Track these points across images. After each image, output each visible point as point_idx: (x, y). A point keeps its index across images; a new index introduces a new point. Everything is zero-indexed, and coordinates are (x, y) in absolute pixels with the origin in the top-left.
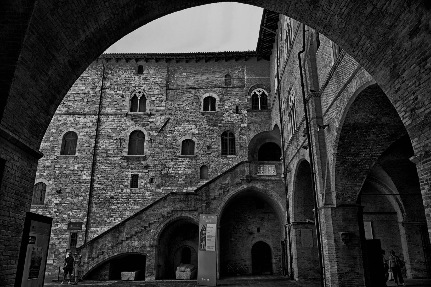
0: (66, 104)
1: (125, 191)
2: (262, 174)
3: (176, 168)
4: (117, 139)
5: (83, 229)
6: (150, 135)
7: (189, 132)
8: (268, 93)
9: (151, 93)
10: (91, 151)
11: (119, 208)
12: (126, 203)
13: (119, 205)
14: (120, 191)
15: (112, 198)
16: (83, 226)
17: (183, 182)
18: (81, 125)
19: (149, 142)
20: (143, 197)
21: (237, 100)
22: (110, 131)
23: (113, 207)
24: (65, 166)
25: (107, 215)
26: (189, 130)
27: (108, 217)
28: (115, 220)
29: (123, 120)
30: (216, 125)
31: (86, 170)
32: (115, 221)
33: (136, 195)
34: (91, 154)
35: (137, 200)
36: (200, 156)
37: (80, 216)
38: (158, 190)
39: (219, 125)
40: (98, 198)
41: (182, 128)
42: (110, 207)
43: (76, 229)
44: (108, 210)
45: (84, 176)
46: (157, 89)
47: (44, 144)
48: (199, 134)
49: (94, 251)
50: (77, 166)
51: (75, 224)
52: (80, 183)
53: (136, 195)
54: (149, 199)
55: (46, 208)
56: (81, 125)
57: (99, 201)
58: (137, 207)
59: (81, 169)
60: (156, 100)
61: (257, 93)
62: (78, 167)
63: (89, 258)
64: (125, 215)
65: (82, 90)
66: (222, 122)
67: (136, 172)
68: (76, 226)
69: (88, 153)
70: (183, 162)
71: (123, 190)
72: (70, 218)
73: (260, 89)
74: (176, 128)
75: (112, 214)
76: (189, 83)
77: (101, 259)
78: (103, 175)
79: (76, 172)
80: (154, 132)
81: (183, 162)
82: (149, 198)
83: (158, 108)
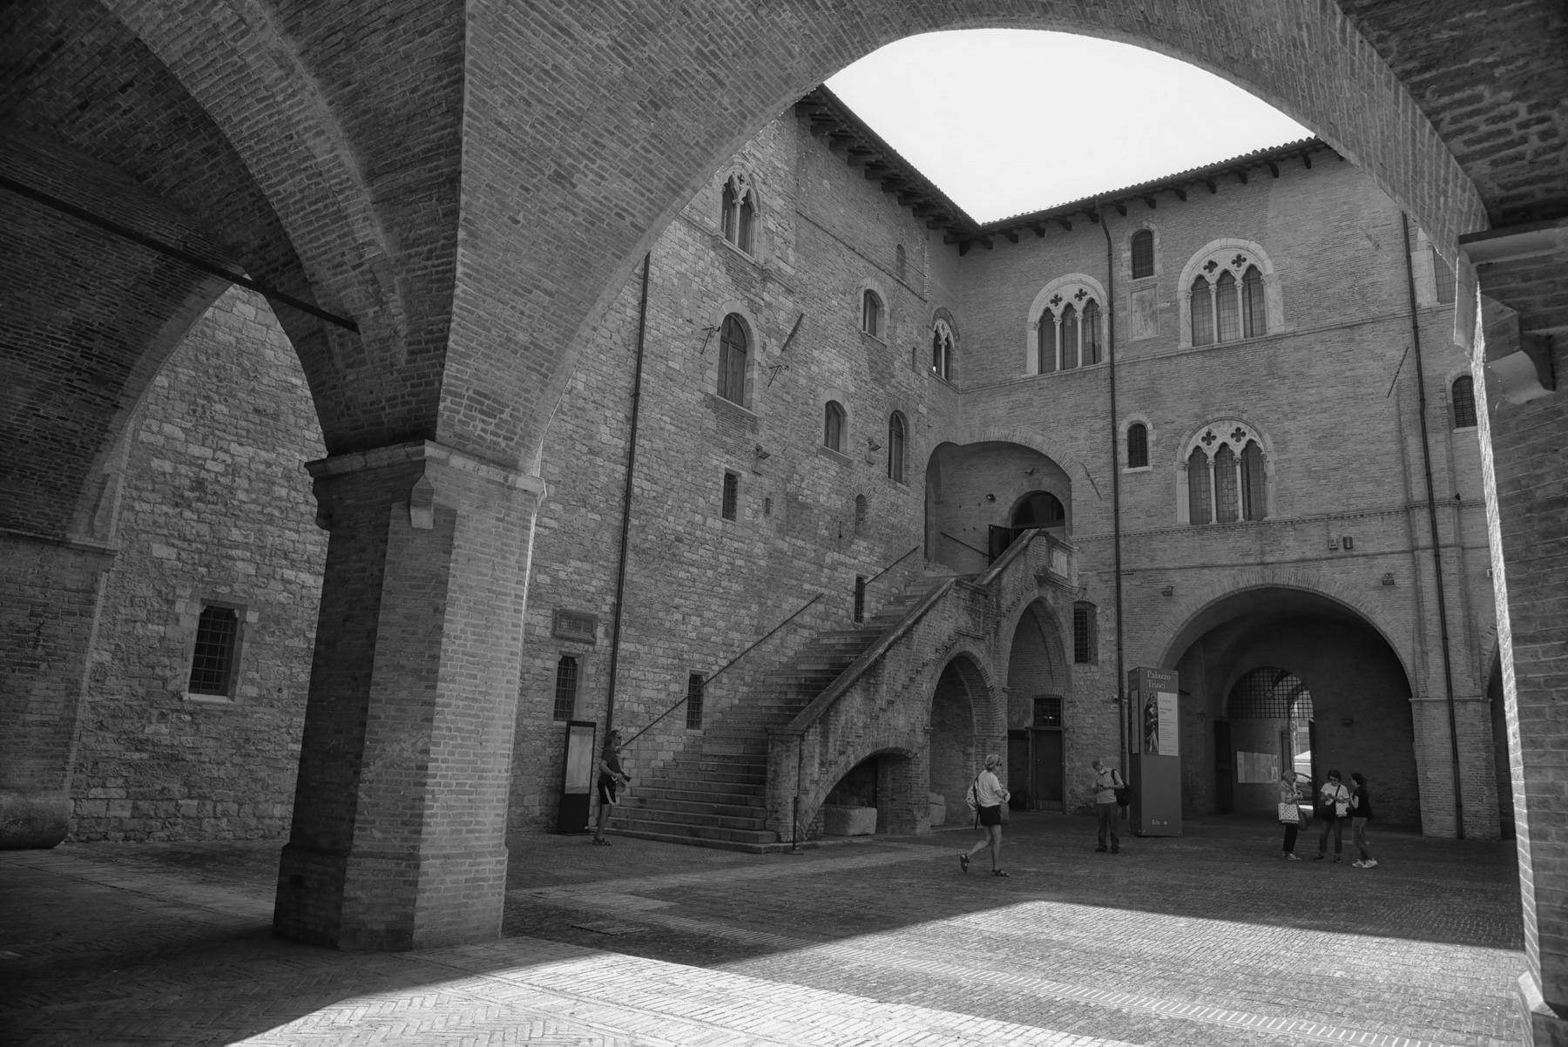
1: (710, 521)
4: (690, 321)
5: (599, 641)
6: (764, 348)
7: (839, 381)
9: (766, 199)
10: (624, 334)
13: (695, 571)
14: (698, 518)
15: (679, 540)
16: (600, 631)
17: (826, 533)
19: (763, 372)
20: (748, 556)
22: (675, 281)
25: (666, 600)
27: (668, 608)
30: (883, 387)
31: (611, 405)
32: (683, 628)
33: (736, 545)
35: (738, 562)
37: (592, 589)
38: (780, 544)
42: (674, 572)
43: (579, 641)
44: (668, 582)
45: (603, 428)
48: (853, 395)
49: (831, 739)
52: (591, 452)
53: (736, 545)
57: (646, 540)
58: (736, 587)
59: (597, 397)
63: (822, 764)
67: (735, 468)
68: (577, 628)
69: (616, 337)
71: (705, 518)
72: (560, 590)
74: (816, 353)
75: (677, 601)
76: (835, 221)
79: (580, 402)
82: (763, 563)
83: (782, 264)
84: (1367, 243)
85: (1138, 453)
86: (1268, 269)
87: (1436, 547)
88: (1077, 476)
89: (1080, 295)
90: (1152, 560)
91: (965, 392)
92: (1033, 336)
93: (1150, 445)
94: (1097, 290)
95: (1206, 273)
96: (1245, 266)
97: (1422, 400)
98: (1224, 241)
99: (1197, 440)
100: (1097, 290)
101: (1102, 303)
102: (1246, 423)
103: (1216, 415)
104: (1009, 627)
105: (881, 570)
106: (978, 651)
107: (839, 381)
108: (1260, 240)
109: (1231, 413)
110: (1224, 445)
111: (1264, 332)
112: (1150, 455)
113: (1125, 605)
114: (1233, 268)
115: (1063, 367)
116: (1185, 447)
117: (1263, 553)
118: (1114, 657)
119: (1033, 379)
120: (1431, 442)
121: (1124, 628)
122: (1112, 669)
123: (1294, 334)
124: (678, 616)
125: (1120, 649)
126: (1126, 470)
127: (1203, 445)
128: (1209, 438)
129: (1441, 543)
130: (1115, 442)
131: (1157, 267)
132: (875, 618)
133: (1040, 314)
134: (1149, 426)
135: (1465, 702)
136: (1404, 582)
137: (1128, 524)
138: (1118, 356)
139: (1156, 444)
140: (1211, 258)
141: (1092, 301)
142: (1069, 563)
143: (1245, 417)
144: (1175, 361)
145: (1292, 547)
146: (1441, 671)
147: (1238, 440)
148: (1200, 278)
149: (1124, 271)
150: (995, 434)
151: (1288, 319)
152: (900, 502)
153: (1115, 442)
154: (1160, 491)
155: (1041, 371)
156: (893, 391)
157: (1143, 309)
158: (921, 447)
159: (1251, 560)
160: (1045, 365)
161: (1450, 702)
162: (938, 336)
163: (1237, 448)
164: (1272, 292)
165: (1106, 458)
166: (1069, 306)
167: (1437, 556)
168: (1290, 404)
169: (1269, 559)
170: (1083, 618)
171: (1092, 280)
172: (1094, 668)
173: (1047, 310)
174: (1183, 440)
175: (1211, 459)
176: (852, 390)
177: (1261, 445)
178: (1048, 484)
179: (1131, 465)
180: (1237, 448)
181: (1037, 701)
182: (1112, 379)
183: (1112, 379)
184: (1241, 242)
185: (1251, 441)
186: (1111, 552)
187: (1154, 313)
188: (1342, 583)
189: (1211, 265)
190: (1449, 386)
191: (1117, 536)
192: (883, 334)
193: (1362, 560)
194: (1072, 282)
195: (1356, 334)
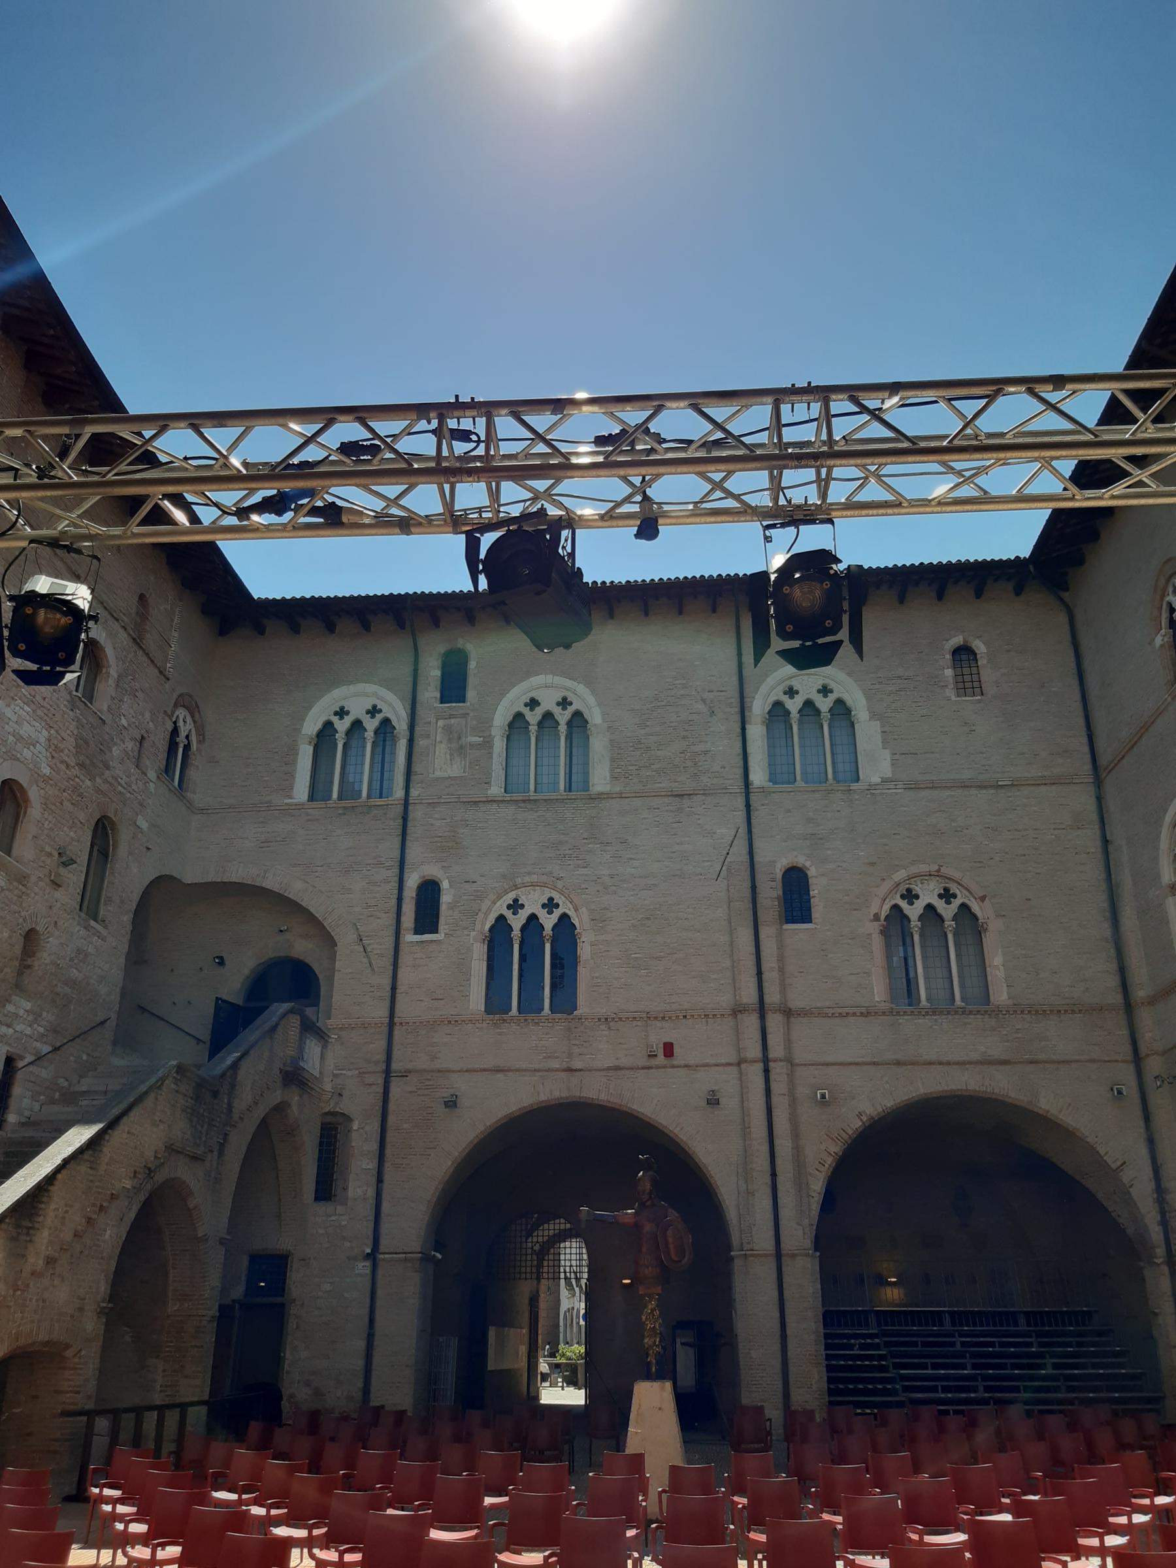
7: (27, 753)
8: (199, 742)
21: (147, 715)
36: (33, 879)
39: (98, 780)
41: (14, 718)
48: (47, 780)
61: (181, 724)
73: (189, 719)
84: (700, 706)
85: (428, 918)
86: (595, 717)
87: (766, 1060)
88: (345, 939)
89: (373, 711)
90: (434, 1058)
91: (202, 811)
92: (305, 754)
93: (443, 908)
94: (396, 710)
95: (526, 711)
96: (571, 710)
97: (754, 888)
98: (549, 679)
99: (501, 908)
100: (396, 710)
101: (401, 724)
102: (561, 893)
103: (527, 879)
104: (239, 1143)
105: (46, 1049)
106: (190, 1176)
107: (27, 753)
108: (588, 684)
109: (544, 879)
110: (533, 918)
111: (586, 788)
112: (442, 920)
113: (391, 1119)
114: (557, 711)
115: (340, 798)
116: (486, 915)
117: (570, 1056)
118: (371, 1192)
119: (300, 806)
120: (762, 936)
121: (388, 1151)
122: (368, 1210)
123: (621, 796)
125: (380, 1181)
126: (409, 937)
127: (508, 914)
128: (515, 906)
129: (771, 1056)
130: (400, 899)
131: (471, 694)
132: (27, 1124)
133: (319, 726)
134: (445, 885)
135: (793, 1256)
136: (730, 1103)
137: (404, 1008)
138: (414, 792)
139: (452, 907)
140: (534, 694)
141: (386, 722)
142: (322, 1057)
143: (560, 884)
144: (483, 807)
145: (603, 1050)
146: (770, 1216)
147: (550, 912)
148: (519, 716)
149: (430, 693)
150: (237, 873)
151: (614, 778)
152: (91, 950)
153: (400, 899)
154: (451, 967)
155: (311, 798)
156: (104, 787)
157: (450, 741)
158: (131, 875)
159: (555, 1064)
160: (317, 791)
161: (779, 1255)
162: (175, 732)
163: (548, 921)
164: (598, 745)
165: (388, 919)
166: (357, 724)
167: (767, 1071)
168: (611, 876)
169: (577, 1065)
170: (331, 1135)
171: (390, 696)
172: (340, 1209)
173: (328, 725)
174: (488, 902)
175: (516, 933)
176: (47, 771)
177: (576, 921)
178: (302, 948)
179: (418, 930)
180: (548, 921)
181: (255, 1259)
182: (405, 819)
183: (405, 819)
184: (569, 683)
185: (564, 917)
186: (382, 1044)
187: (462, 747)
188: (658, 1099)
189: (533, 703)
190: (779, 875)
191: (391, 1025)
192: (102, 704)
193: (683, 1071)
194: (366, 695)
195: (686, 802)
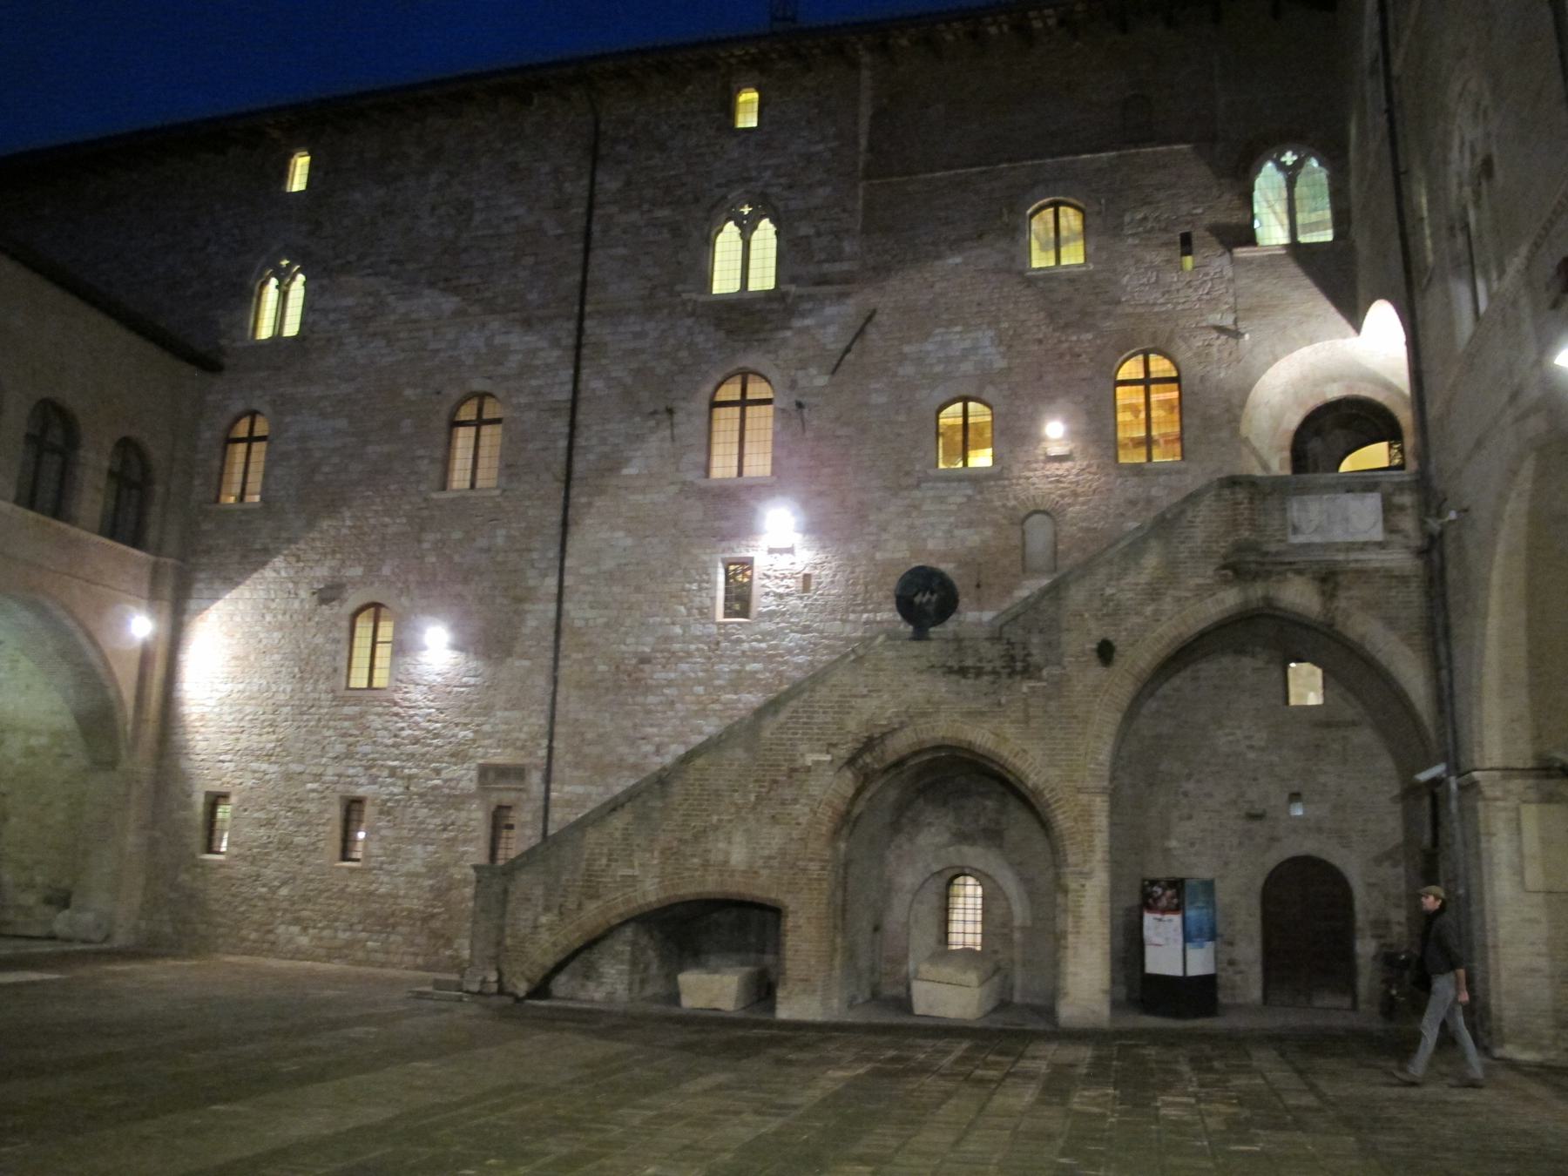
0: (454, 283)
2: (1317, 539)
3: (911, 527)
6: (793, 385)
11: (673, 703)
12: (699, 682)
15: (644, 660)
18: (514, 361)
23: (651, 699)
24: (457, 535)
26: (965, 355)
28: (658, 752)
29: (682, 332)
34: (557, 480)
37: (523, 736)
40: (589, 660)
46: (821, 183)
47: (378, 449)
50: (501, 532)
51: (503, 772)
54: (798, 667)
55: (396, 704)
56: (514, 361)
60: (819, 234)
62: (509, 537)
64: (701, 733)
65: (516, 218)
66: (1119, 310)
70: (942, 500)
74: (907, 349)
77: (593, 915)
78: (604, 568)
80: (813, 371)
81: (942, 500)
124: (649, 748)
176: (1001, 363)
